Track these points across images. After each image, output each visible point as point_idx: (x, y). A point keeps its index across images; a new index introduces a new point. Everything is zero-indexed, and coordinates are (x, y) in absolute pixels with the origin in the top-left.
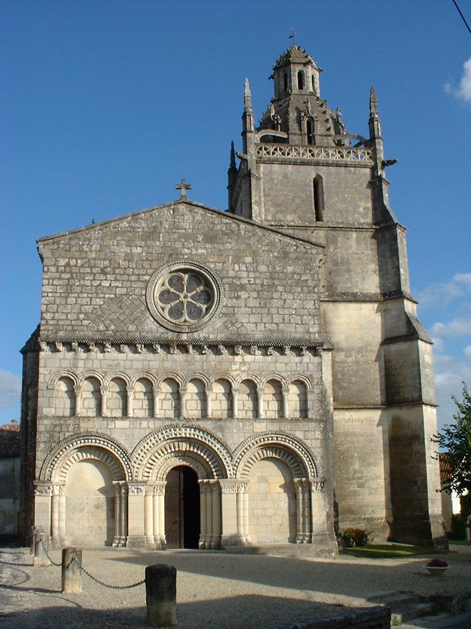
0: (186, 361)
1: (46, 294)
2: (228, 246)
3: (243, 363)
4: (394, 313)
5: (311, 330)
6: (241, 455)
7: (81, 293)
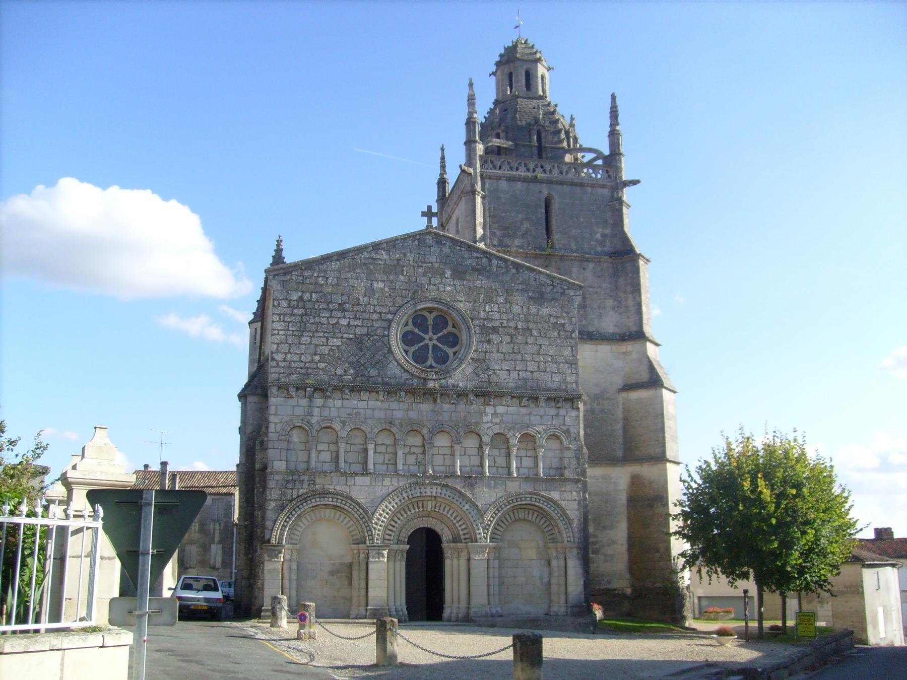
0: (433, 411)
1: (276, 332)
2: (478, 283)
3: (495, 414)
4: (635, 356)
5: (569, 379)
7: (317, 331)
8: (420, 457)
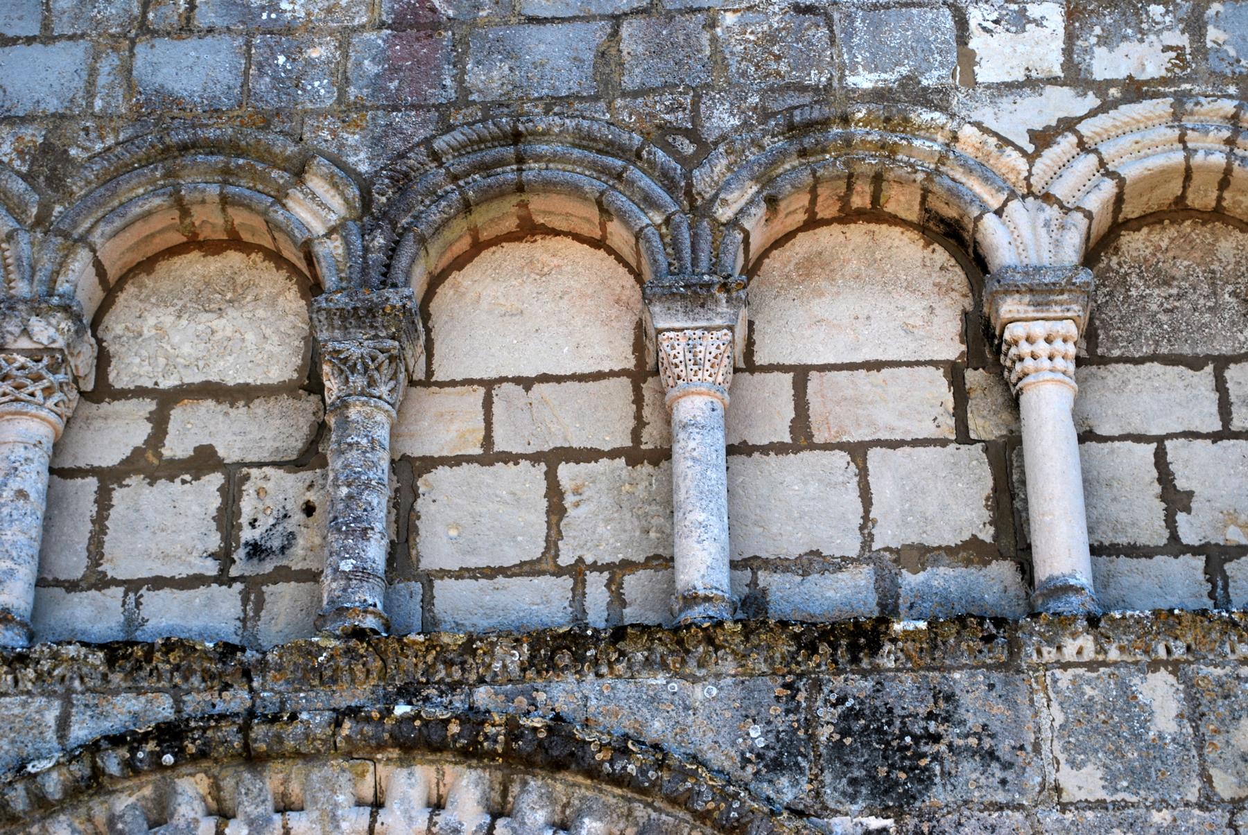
8: (272, 497)
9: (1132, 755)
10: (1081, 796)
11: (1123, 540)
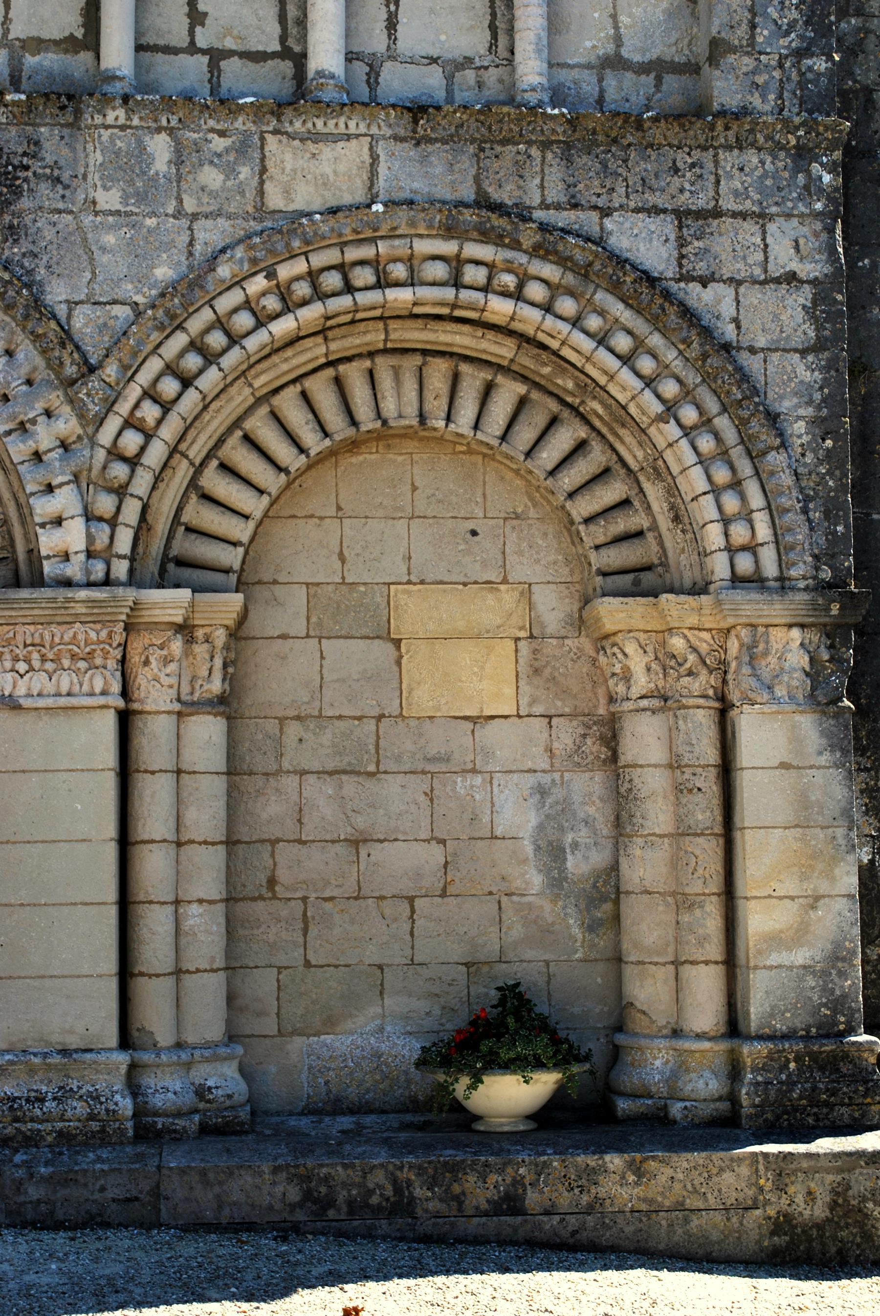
6: (150, 394)
9: (139, 184)
10: (107, 207)
11: (161, 42)
